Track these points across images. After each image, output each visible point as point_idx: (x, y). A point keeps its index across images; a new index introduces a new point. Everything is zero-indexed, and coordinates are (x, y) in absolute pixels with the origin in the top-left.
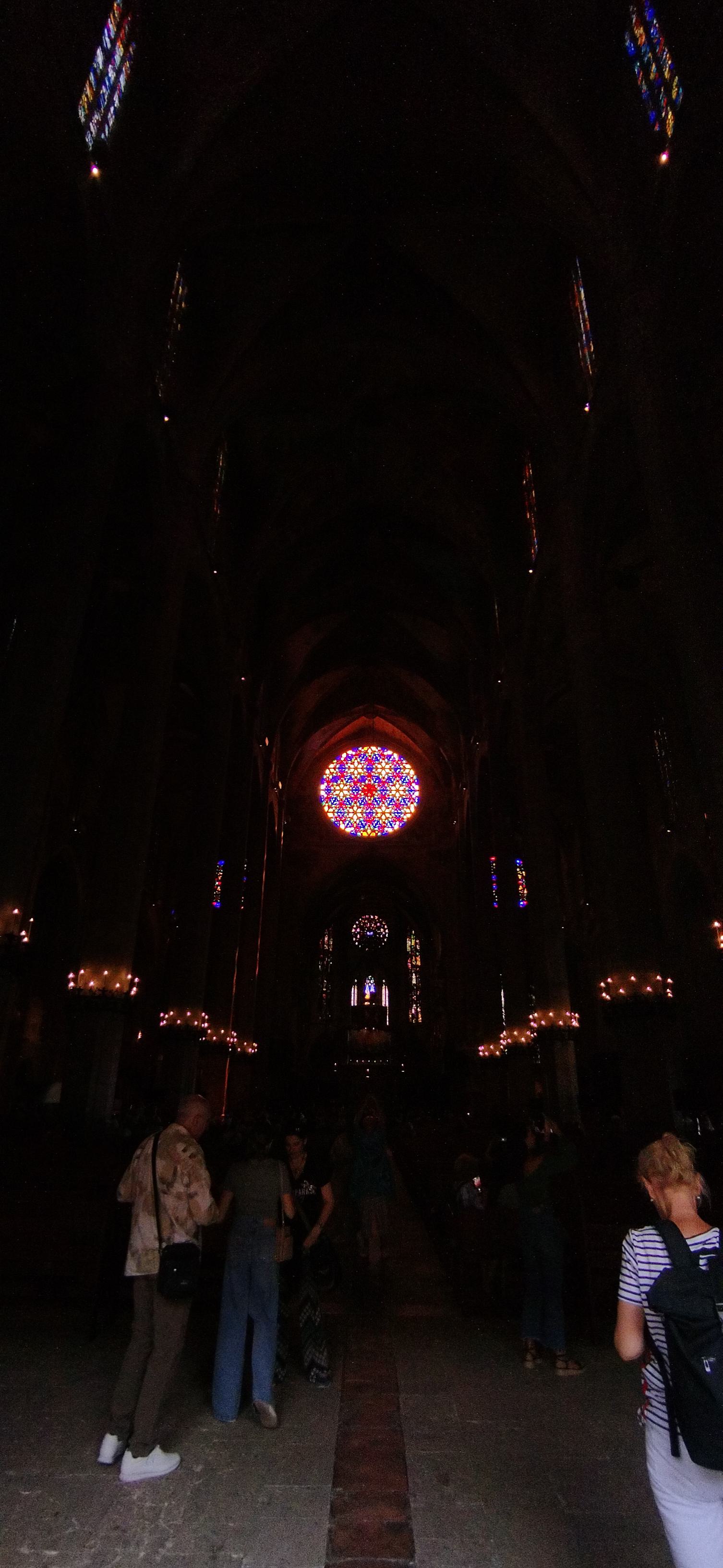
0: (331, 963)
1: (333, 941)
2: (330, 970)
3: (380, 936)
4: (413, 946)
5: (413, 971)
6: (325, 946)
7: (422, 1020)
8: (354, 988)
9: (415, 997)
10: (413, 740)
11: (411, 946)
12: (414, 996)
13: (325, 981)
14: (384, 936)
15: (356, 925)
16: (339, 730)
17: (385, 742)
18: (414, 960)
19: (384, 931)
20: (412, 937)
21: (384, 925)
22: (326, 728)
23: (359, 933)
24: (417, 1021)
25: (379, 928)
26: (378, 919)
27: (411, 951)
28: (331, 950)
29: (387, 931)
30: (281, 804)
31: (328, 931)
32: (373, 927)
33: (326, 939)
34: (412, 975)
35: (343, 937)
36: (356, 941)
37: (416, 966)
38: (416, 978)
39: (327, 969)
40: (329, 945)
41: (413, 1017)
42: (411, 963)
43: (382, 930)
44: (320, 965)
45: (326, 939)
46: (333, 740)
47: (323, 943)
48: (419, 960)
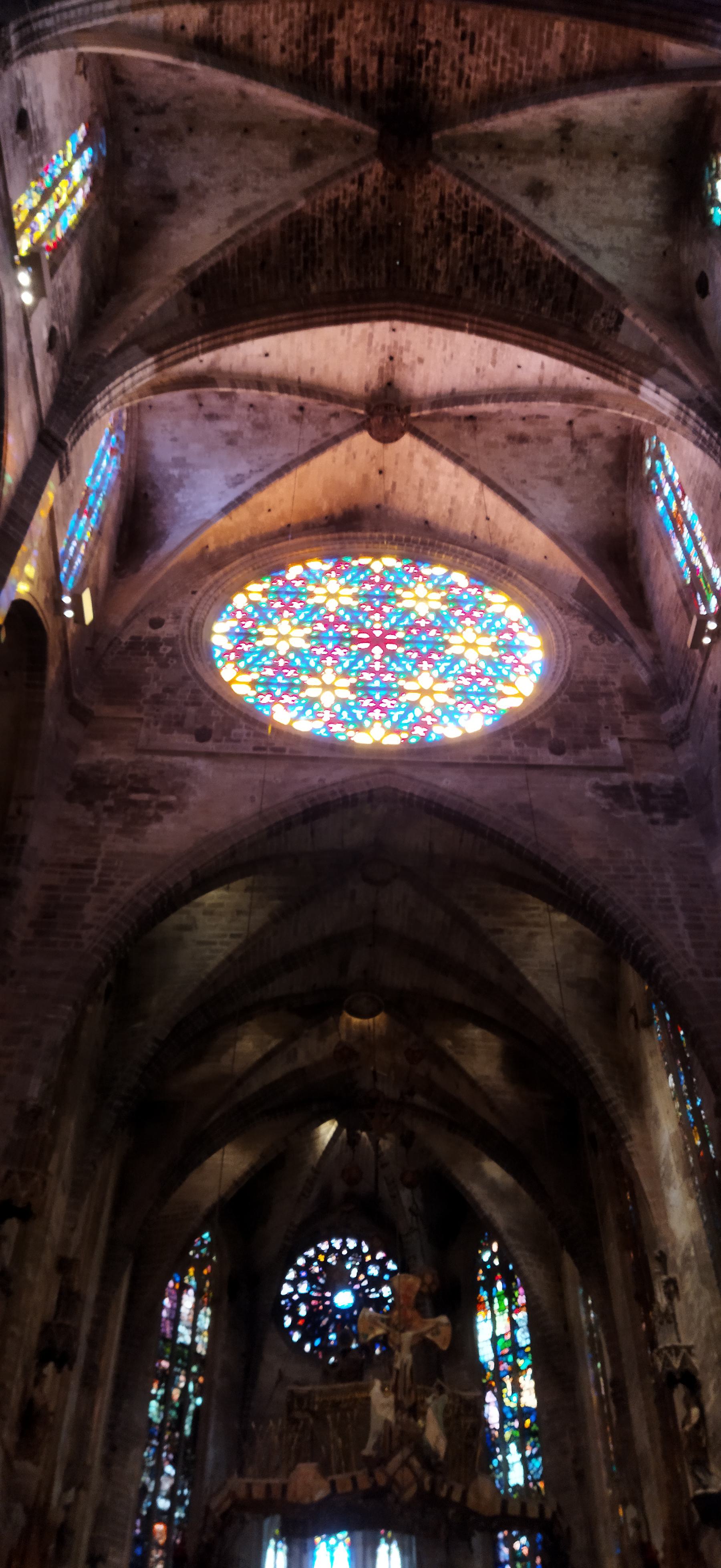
0: (199, 1401)
4: (502, 1336)
5: (507, 1435)
10: (522, 510)
11: (494, 1339)
13: (169, 1469)
15: (298, 1269)
16: (286, 469)
18: (508, 1390)
20: (496, 1306)
23: (305, 1298)
27: (497, 1360)
34: (505, 1452)
36: (294, 1327)
38: (525, 1461)
39: (179, 1425)
42: (501, 1404)
44: (154, 1397)
47: (176, 1319)
48: (532, 1384)
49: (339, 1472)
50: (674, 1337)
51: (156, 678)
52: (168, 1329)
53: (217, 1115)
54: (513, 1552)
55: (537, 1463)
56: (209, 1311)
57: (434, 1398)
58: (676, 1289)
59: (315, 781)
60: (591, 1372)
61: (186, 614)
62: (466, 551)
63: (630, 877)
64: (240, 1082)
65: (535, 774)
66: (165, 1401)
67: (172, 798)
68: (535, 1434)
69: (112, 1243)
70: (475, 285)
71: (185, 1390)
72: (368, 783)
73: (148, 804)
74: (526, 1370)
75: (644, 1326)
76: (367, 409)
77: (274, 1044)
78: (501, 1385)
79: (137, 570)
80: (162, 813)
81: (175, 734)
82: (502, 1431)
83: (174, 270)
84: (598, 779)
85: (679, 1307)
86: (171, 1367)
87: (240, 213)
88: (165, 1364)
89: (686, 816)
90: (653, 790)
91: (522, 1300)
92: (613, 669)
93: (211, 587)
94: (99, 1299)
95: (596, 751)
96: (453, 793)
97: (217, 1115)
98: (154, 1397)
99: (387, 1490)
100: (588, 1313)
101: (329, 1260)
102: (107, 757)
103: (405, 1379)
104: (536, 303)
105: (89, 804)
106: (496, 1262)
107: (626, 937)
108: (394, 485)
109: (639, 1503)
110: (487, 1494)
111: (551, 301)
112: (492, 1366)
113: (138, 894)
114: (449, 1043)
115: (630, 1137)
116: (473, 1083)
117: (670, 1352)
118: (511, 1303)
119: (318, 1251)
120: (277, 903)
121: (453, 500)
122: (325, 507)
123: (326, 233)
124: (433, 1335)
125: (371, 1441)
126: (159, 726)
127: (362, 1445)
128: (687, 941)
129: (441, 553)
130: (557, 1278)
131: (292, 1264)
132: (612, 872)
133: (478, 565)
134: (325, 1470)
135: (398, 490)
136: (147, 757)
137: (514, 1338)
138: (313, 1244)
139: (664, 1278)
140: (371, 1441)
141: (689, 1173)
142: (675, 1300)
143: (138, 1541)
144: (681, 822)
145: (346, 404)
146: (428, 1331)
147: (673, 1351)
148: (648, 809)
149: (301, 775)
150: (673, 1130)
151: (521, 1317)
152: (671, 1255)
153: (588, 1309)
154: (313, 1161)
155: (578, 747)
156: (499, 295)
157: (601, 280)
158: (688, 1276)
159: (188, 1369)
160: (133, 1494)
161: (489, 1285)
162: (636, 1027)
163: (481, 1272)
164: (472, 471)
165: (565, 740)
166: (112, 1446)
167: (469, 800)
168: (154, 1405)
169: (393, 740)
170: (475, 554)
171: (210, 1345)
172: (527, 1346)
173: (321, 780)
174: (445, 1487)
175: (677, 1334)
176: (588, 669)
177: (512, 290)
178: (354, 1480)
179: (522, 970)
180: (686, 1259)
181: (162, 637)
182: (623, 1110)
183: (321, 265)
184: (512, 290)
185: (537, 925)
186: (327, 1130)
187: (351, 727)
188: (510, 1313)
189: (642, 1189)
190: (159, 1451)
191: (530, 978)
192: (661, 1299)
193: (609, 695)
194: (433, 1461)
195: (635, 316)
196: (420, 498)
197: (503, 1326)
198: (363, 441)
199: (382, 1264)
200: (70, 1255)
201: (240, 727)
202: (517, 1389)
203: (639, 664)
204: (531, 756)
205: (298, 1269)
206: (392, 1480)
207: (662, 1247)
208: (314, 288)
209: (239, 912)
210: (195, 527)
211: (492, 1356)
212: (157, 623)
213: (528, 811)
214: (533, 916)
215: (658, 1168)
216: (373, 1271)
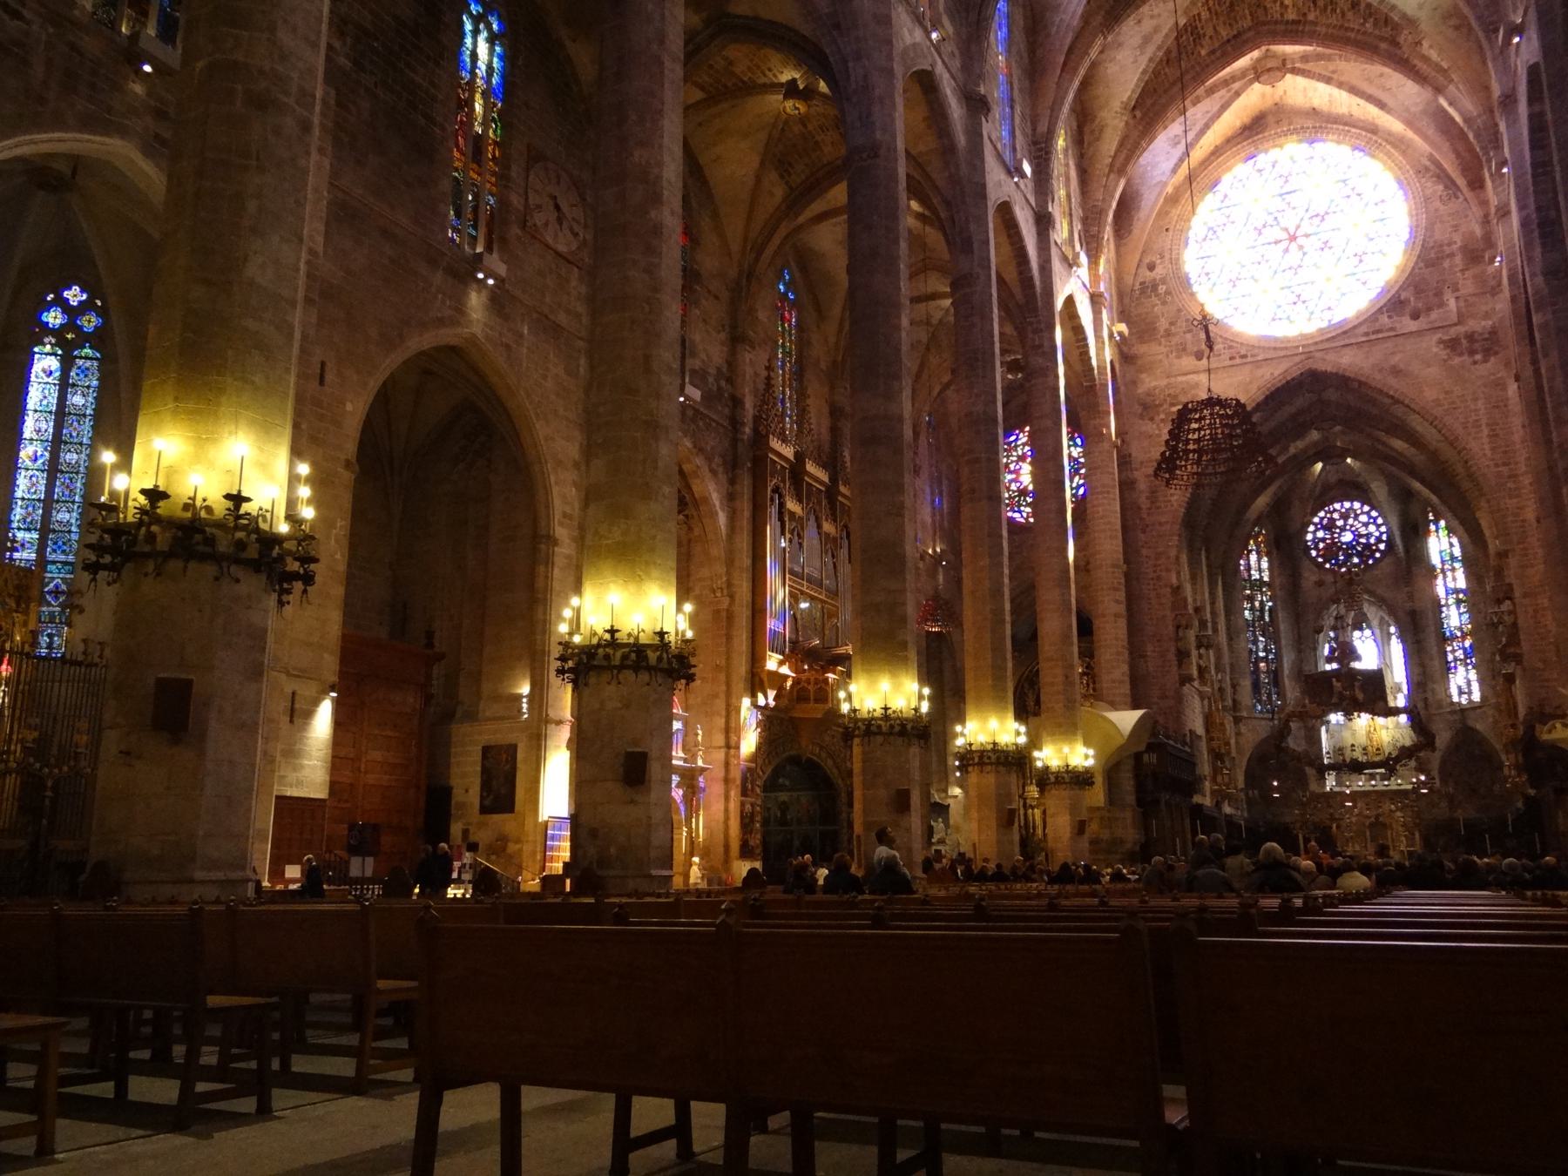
0: (1270, 604)
2: (1270, 616)
3: (1368, 539)
6: (1253, 572)
7: (1482, 697)
9: (1461, 651)
10: (1381, 105)
12: (1456, 651)
13: (1261, 639)
14: (1379, 540)
15: (1316, 525)
16: (1207, 126)
17: (1317, 124)
18: (1449, 579)
19: (1377, 530)
21: (1375, 519)
22: (1176, 128)
23: (1323, 540)
24: (1470, 701)
25: (1366, 525)
26: (1361, 508)
27: (1443, 562)
28: (1266, 579)
29: (1383, 529)
30: (1095, 299)
31: (1257, 544)
32: (1352, 526)
33: (1253, 557)
34: (1448, 610)
35: (1286, 548)
36: (1318, 556)
37: (1457, 591)
39: (1262, 617)
40: (1260, 570)
41: (1461, 693)
42: (1446, 587)
43: (1372, 528)
44: (1246, 609)
45: (1253, 557)
46: (1198, 154)
47: (1249, 568)
48: (1463, 576)
51: (1163, 316)
52: (1246, 575)
55: (1467, 616)
56: (1266, 559)
59: (1268, 376)
61: (1167, 256)
62: (1347, 128)
65: (1401, 340)
66: (1252, 609)
68: (1464, 602)
70: (1315, 11)
71: (1262, 602)
76: (1255, 73)
78: (1445, 577)
79: (1130, 232)
82: (1447, 599)
83: (1116, 105)
87: (1146, 40)
88: (1248, 592)
89: (1496, 353)
92: (1456, 228)
93: (1177, 222)
94: (1210, 593)
98: (1246, 609)
102: (1154, 384)
104: (1362, 21)
105: (1152, 419)
108: (1285, 92)
111: (1372, 20)
112: (1439, 566)
121: (1330, 95)
122: (1238, 124)
123: (1203, 17)
128: (1487, 447)
129: (1328, 133)
133: (1357, 138)
135: (1288, 93)
136: (1173, 380)
143: (1253, 673)
144: (1492, 359)
145: (1239, 79)
148: (1472, 352)
149: (1260, 372)
154: (1312, 480)
155: (1429, 309)
156: (1334, 16)
157: (1404, 16)
159: (1261, 591)
160: (1245, 654)
164: (1340, 85)
166: (1230, 639)
168: (1247, 613)
170: (1353, 130)
171: (1271, 576)
173: (1272, 374)
176: (1438, 236)
177: (1343, 14)
181: (1158, 277)
183: (1204, 35)
184: (1343, 14)
186: (1319, 466)
190: (1254, 632)
193: (1452, 255)
195: (1431, 47)
196: (1305, 96)
198: (1256, 86)
199: (1368, 513)
200: (1199, 604)
203: (1474, 221)
204: (1398, 326)
205: (1316, 525)
208: (1203, 52)
210: (1158, 189)
212: (1151, 267)
216: (1364, 518)
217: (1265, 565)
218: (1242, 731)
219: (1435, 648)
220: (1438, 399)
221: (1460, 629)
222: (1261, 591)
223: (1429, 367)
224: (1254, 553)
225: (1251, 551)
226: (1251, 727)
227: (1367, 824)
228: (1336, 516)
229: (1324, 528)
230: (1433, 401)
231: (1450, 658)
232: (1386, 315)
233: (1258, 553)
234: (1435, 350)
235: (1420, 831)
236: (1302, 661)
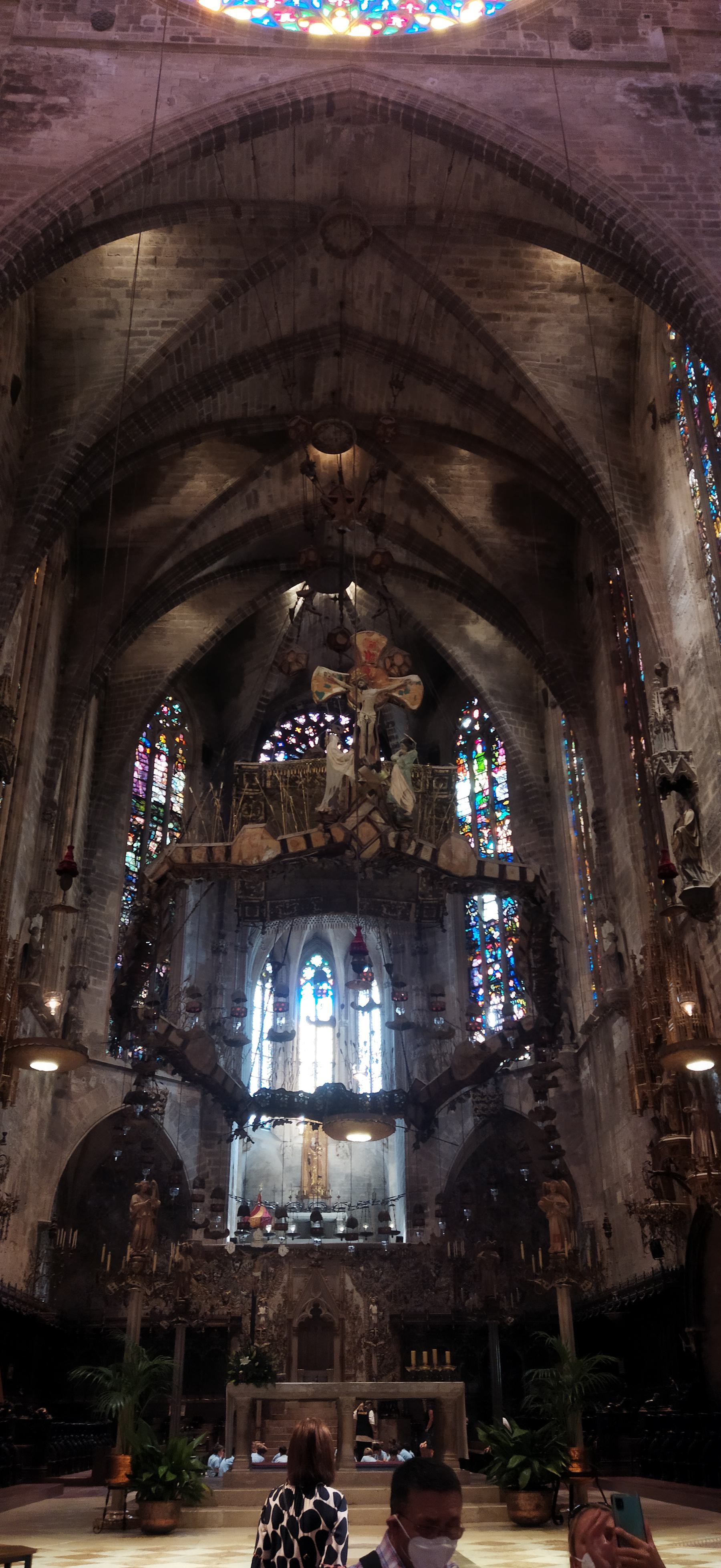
1: (185, 781)
6: (154, 789)
8: (263, 989)
9: (497, 967)
28: (177, 808)
33: (161, 765)
44: (131, 849)
45: (161, 765)
49: (291, 830)
50: (671, 742)
53: (168, 564)
54: (486, 977)
56: (183, 776)
57: (400, 755)
58: (677, 698)
60: (571, 814)
63: (668, 197)
64: (193, 526)
66: (141, 852)
67: (63, 100)
69: (62, 690)
72: (326, 84)
73: (31, 107)
74: (504, 820)
75: (633, 754)
77: (230, 483)
80: (49, 118)
81: (65, 21)
84: (632, 80)
85: (678, 716)
86: (145, 824)
88: (140, 820)
90: (704, 93)
91: (502, 759)
94: (52, 742)
95: (631, 45)
96: (439, 96)
97: (168, 564)
99: (345, 845)
100: (571, 760)
101: (307, 732)
103: (367, 736)
106: (477, 727)
107: (659, 272)
109: (615, 919)
110: (461, 854)
112: (469, 820)
113: (22, 216)
114: (431, 480)
115: (636, 550)
116: (457, 525)
117: (665, 757)
118: (490, 763)
119: (295, 724)
120: (217, 280)
124: (401, 693)
125: (327, 797)
126: (42, 11)
127: (319, 799)
130: (540, 733)
131: (266, 735)
132: (646, 192)
134: (274, 830)
137: (493, 793)
138: (290, 718)
139: (663, 689)
140: (327, 797)
141: (705, 571)
142: (675, 710)
146: (395, 689)
147: (669, 757)
149: (237, 71)
150: (689, 531)
151: (501, 775)
152: (673, 666)
153: (571, 756)
158: (693, 681)
159: (164, 826)
161: (469, 749)
162: (654, 427)
163: (461, 737)
165: (591, 30)
167: (462, 105)
168: (130, 856)
169: (362, 32)
172: (506, 799)
174: (413, 844)
175: (675, 741)
178: (307, 838)
179: (522, 365)
180: (691, 667)
182: (630, 523)
185: (542, 309)
187: (305, 15)
188: (490, 770)
189: (646, 602)
191: (529, 374)
192: (658, 709)
194: (399, 817)
197: (483, 780)
201: (154, 12)
202: (494, 838)
206: (351, 835)
207: (664, 659)
209: (171, 294)
211: (469, 811)
213: (536, 118)
214: (537, 297)
215: (666, 580)
217: (179, 784)
218: (73, 1088)
219: (452, 961)
220: (625, 177)
221: (499, 924)
222: (164, 826)
223: (609, 122)
224: (163, 757)
225: (160, 753)
226: (92, 1084)
227: (295, 1324)
228: (309, 732)
229: (289, 749)
230: (618, 178)
231: (478, 979)
232: (521, 33)
233: (171, 759)
234: (620, 98)
235: (574, 1292)
236: (218, 969)
